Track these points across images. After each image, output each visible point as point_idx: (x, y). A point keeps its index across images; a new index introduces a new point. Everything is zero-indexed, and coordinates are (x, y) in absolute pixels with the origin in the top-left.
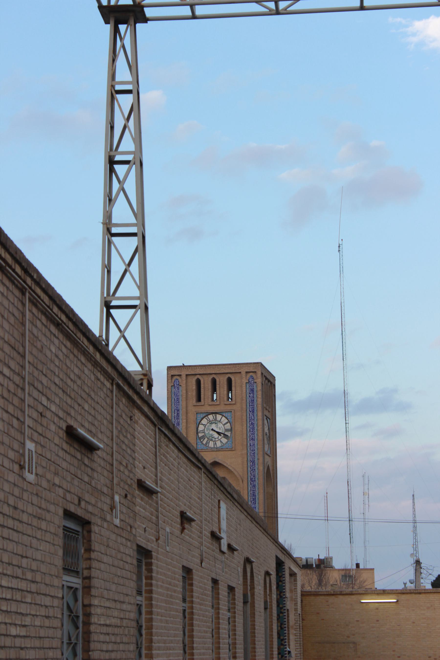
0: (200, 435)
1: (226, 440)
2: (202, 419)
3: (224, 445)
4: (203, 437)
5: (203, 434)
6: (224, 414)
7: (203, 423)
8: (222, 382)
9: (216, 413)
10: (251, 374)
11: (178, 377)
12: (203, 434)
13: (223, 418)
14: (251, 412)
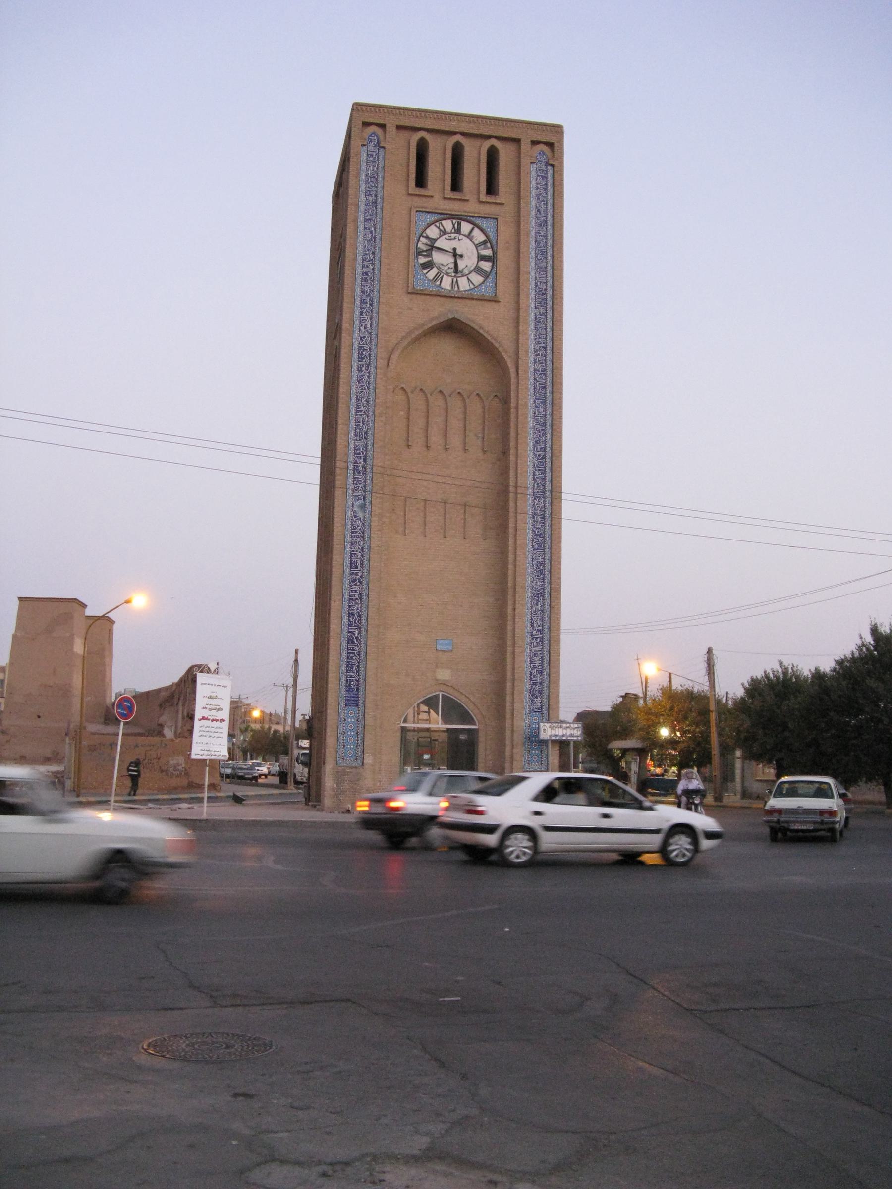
1: (481, 279)
2: (429, 226)
6: (478, 221)
7: (431, 236)
8: (474, 157)
9: (461, 218)
11: (379, 131)
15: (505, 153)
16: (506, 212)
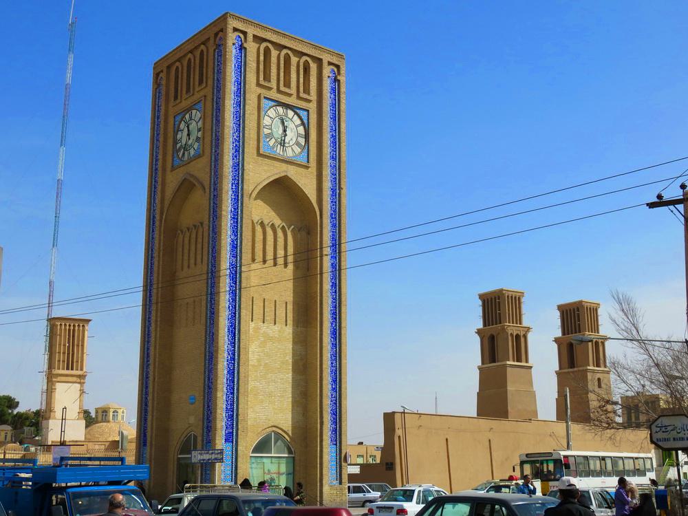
0: (266, 131)
1: (299, 150)
3: (297, 156)
4: (270, 136)
5: (270, 131)
6: (298, 111)
10: (332, 67)
12: (270, 131)
13: (296, 117)
14: (331, 118)
15: (313, 67)
16: (313, 107)
